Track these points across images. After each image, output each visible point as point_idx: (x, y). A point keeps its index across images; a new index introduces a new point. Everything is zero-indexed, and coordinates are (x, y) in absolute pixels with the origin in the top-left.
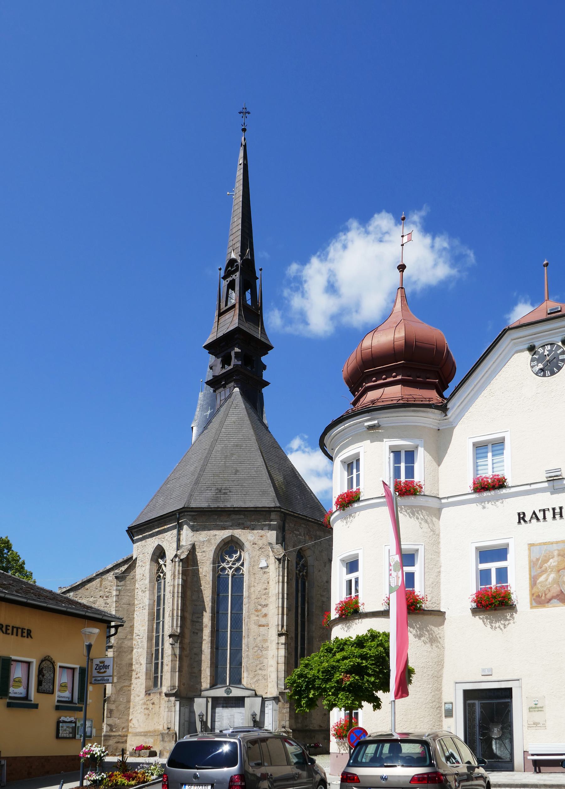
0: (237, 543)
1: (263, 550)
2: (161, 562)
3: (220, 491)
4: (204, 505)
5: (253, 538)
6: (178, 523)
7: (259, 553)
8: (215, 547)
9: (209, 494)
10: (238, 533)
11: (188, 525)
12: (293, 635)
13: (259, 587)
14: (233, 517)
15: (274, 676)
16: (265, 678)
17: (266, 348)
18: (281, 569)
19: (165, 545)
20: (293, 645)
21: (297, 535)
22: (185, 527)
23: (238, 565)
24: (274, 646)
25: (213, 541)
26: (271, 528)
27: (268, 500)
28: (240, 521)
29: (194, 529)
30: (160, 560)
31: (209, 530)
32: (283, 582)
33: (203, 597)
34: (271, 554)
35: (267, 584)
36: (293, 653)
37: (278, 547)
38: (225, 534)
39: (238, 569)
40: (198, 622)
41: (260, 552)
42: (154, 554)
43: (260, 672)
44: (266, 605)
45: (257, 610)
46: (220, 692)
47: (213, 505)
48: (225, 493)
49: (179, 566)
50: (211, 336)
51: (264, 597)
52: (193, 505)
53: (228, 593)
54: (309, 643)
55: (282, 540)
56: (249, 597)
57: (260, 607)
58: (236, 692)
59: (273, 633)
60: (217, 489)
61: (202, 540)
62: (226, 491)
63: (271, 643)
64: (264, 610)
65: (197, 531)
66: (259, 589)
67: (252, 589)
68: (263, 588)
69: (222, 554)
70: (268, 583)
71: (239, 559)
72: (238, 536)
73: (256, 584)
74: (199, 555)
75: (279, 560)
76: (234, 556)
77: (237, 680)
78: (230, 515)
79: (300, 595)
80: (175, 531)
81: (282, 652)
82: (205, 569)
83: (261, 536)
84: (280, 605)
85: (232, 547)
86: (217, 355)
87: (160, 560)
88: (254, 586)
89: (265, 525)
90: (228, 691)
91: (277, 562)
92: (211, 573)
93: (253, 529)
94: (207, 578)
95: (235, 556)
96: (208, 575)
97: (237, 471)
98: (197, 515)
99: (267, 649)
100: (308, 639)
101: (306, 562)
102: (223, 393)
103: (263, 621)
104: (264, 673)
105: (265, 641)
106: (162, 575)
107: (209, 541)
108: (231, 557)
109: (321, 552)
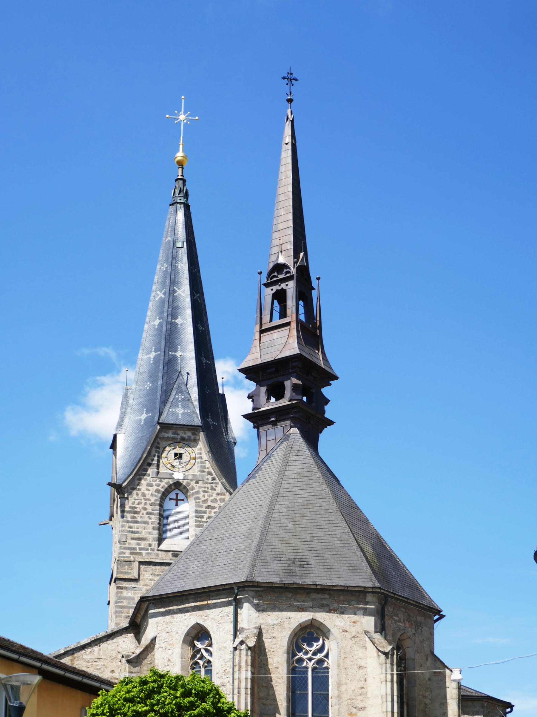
0: (319, 629)
1: (357, 639)
2: (199, 645)
3: (294, 562)
4: (275, 579)
5: (342, 624)
6: (235, 599)
7: (351, 642)
8: (289, 633)
9: (280, 566)
10: (322, 617)
11: (251, 603)
13: (354, 686)
14: (314, 596)
18: (389, 666)
19: (209, 625)
22: (246, 605)
23: (319, 656)
25: (286, 625)
26: (367, 612)
27: (364, 578)
28: (324, 602)
29: (259, 608)
30: (196, 643)
31: (281, 610)
32: (392, 681)
33: (274, 694)
34: (369, 644)
35: (363, 682)
37: (378, 637)
38: (304, 617)
39: (320, 662)
41: (354, 642)
42: (188, 634)
44: (363, 708)
47: (288, 581)
48: (301, 566)
49: (247, 655)
50: (249, 357)
51: (360, 697)
52: (259, 579)
53: (307, 690)
55: (381, 628)
56: (339, 697)
57: (354, 711)
60: (289, 560)
61: (271, 622)
62: (302, 563)
65: (264, 611)
66: (353, 688)
67: (344, 688)
68: (359, 686)
70: (366, 681)
71: (321, 649)
72: (321, 620)
73: (348, 682)
74: (268, 642)
75: (386, 654)
76: (315, 644)
78: (309, 593)
80: (230, 609)
82: (276, 659)
83: (354, 622)
84: (389, 709)
85: (311, 634)
86: (259, 383)
87: (196, 643)
88: (346, 684)
89: (360, 609)
91: (383, 657)
92: (285, 665)
93: (342, 613)
94: (280, 670)
95: (316, 646)
96: (280, 667)
97: (312, 539)
98: (262, 591)
102: (273, 433)
106: (201, 662)
107: (281, 624)
108: (310, 645)
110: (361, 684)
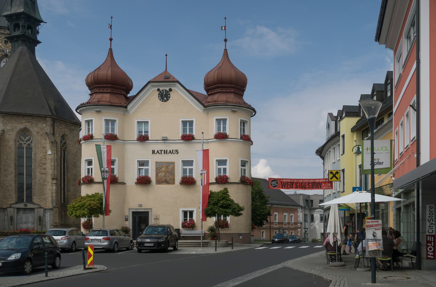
12: (59, 179)
13: (41, 155)
14: (26, 118)
15: (50, 199)
16: (45, 199)
17: (39, 21)
20: (59, 183)
21: (61, 129)
23: (29, 142)
24: (50, 184)
34: (47, 139)
36: (60, 188)
39: (29, 145)
40: (7, 170)
43: (42, 196)
45: (40, 166)
46: (21, 205)
54: (67, 182)
56: (35, 159)
57: (41, 165)
58: (30, 206)
59: (49, 178)
61: (8, 128)
63: (48, 182)
64: (44, 166)
67: (37, 155)
69: (20, 137)
71: (29, 140)
74: (7, 136)
77: (30, 199)
79: (62, 158)
81: (54, 188)
90: (26, 205)
99: (46, 185)
100: (67, 180)
101: (66, 141)
103: (43, 171)
104: (44, 197)
105: (45, 181)
107: (12, 129)
109: (74, 137)
110: (44, 154)
